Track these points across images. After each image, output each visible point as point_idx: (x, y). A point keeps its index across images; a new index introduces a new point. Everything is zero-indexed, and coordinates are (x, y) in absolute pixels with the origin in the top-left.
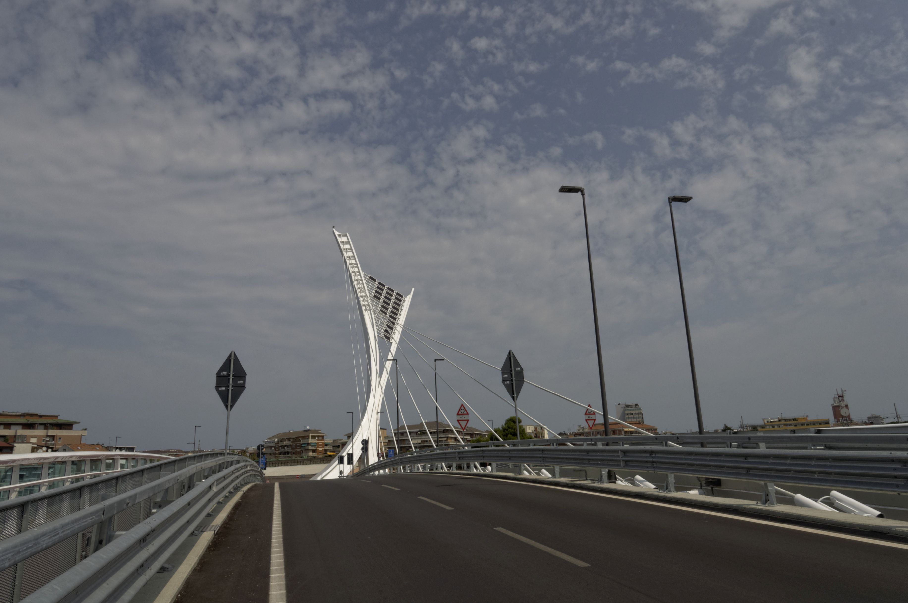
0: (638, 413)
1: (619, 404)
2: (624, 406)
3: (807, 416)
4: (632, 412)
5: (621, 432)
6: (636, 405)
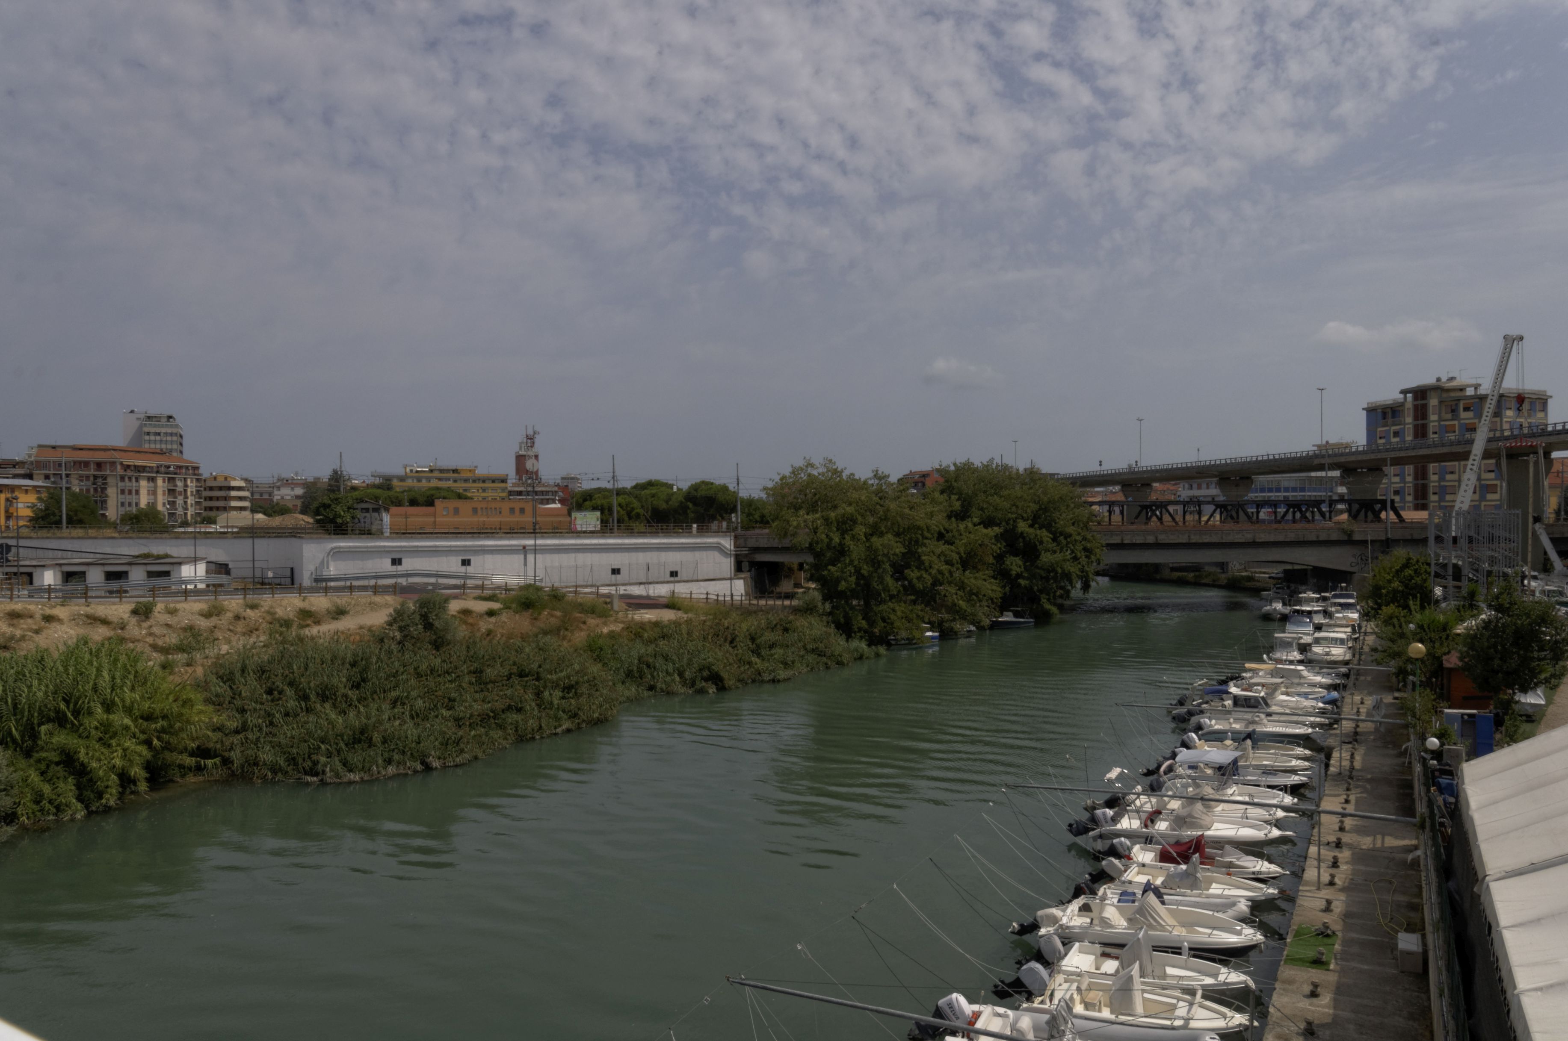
0: (171, 434)
1: (132, 412)
2: (142, 416)
3: (476, 467)
4: (158, 430)
5: (116, 468)
6: (170, 417)
